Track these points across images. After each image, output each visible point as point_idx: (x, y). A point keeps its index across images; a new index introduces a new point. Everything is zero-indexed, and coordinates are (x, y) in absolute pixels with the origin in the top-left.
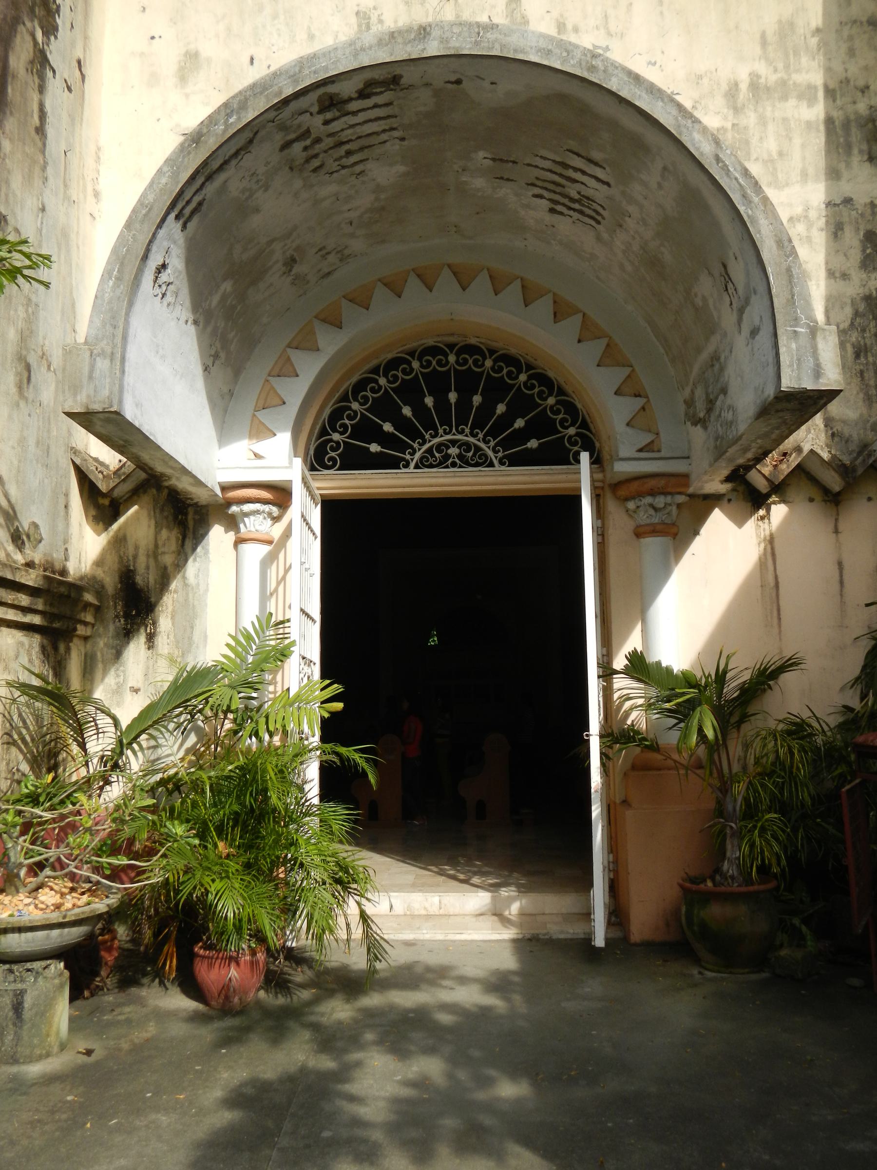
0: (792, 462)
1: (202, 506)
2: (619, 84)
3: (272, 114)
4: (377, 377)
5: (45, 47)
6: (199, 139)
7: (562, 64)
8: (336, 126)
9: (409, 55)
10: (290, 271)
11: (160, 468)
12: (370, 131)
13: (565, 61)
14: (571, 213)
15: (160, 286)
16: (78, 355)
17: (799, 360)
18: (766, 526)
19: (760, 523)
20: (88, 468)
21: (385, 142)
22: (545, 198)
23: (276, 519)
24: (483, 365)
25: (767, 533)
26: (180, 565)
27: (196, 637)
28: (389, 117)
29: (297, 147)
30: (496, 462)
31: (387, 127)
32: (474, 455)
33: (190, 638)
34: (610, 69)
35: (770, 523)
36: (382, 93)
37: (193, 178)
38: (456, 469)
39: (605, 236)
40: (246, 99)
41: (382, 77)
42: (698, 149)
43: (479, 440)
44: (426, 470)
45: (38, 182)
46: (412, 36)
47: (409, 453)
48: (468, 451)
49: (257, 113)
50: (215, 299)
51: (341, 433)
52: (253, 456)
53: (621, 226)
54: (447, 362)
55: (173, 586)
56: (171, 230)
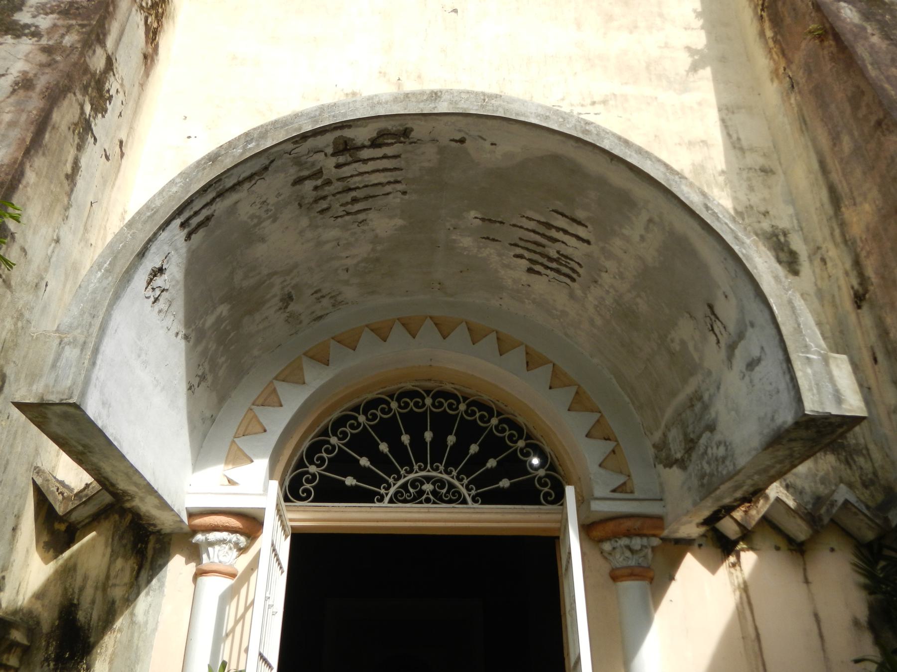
0: (761, 508)
1: (165, 534)
2: (611, 145)
3: (290, 146)
4: (357, 415)
5: (91, 119)
6: (216, 158)
8: (347, 171)
9: (422, 110)
10: (286, 307)
11: (122, 484)
12: (376, 182)
13: (560, 125)
14: (548, 272)
15: (153, 289)
16: (45, 342)
17: (817, 385)
18: (738, 573)
19: (732, 570)
20: (48, 487)
21: (388, 194)
22: (525, 258)
23: (242, 550)
24: (457, 408)
25: (741, 580)
26: (129, 600)
28: (395, 169)
29: (309, 185)
30: (469, 499)
31: (392, 180)
32: (448, 492)
34: (602, 134)
35: (741, 570)
36: (392, 144)
37: (204, 190)
38: (429, 505)
39: (579, 293)
40: (267, 131)
41: (394, 129)
42: (688, 198)
43: (453, 478)
44: (400, 505)
45: (57, 216)
46: (425, 98)
47: (384, 488)
48: (442, 487)
50: (210, 320)
51: (318, 466)
52: (227, 483)
53: (596, 282)
54: (424, 405)
55: (118, 624)
56: (174, 236)
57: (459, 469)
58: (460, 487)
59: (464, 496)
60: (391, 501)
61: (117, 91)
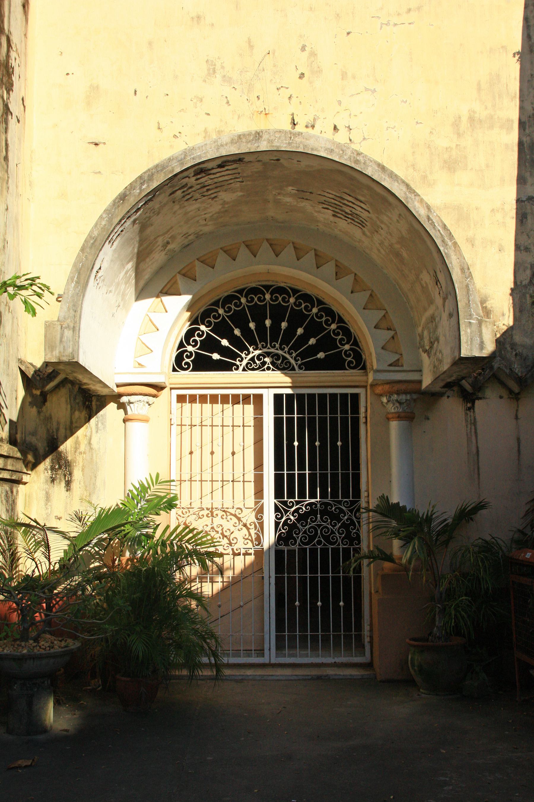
1: (102, 396)
4: (218, 309)
7: (341, 157)
9: (250, 149)
10: (166, 248)
14: (347, 219)
16: (54, 328)
17: (471, 339)
18: (472, 414)
19: (468, 412)
21: (231, 183)
22: (330, 210)
24: (288, 301)
27: (99, 483)
29: (179, 193)
30: (296, 367)
32: (282, 362)
33: (94, 484)
34: (368, 162)
35: (474, 412)
36: (232, 165)
38: (270, 372)
39: (368, 234)
40: (153, 174)
42: (417, 212)
43: (285, 353)
46: (251, 138)
47: (239, 360)
48: (278, 359)
49: (159, 183)
52: (137, 365)
54: (265, 299)
57: (290, 346)
58: (290, 359)
59: (293, 365)
60: (244, 370)
61: (15, 59)
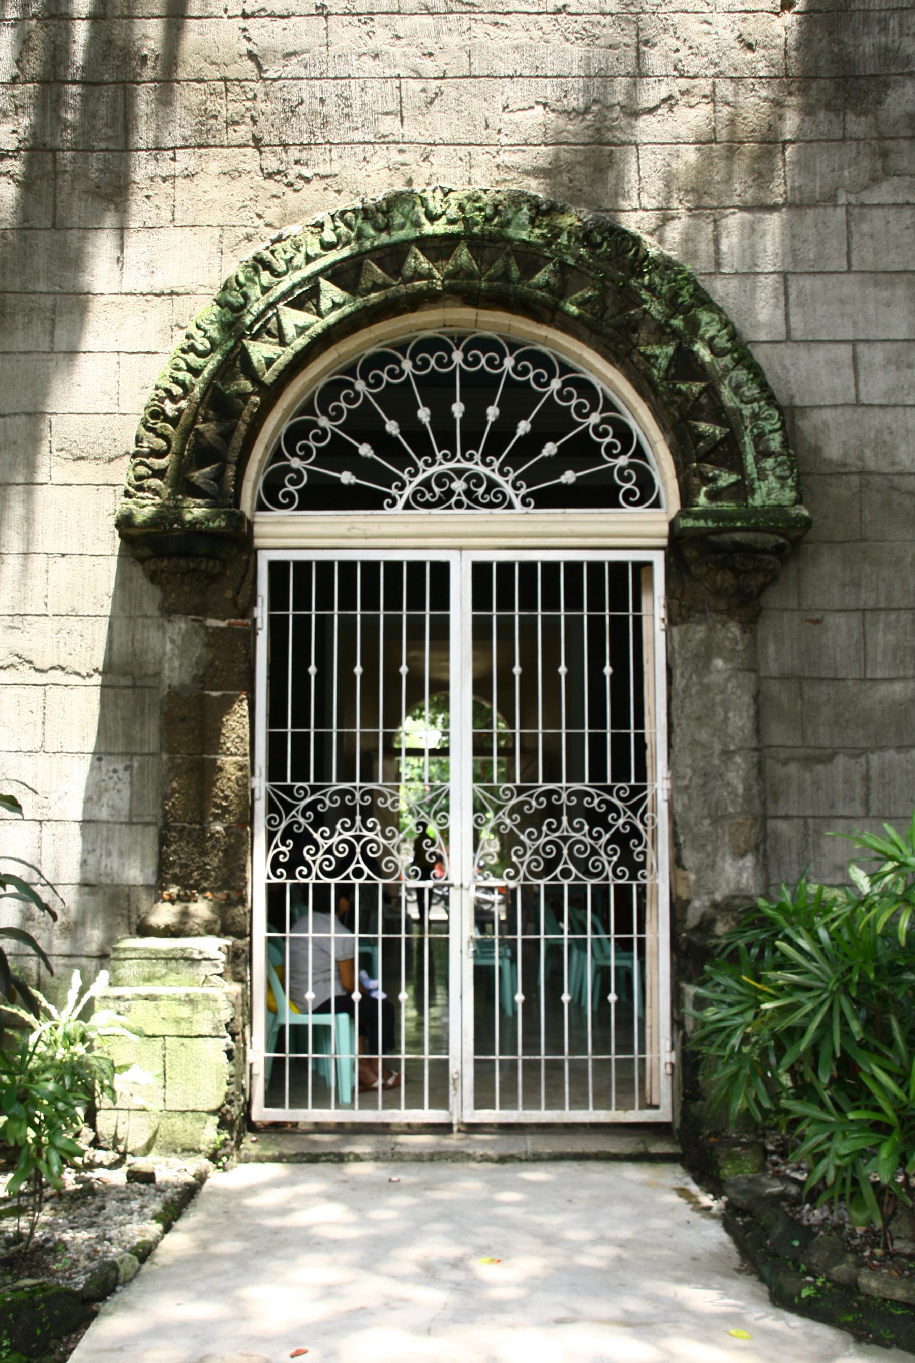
30: (517, 502)
32: (487, 491)
38: (462, 511)
47: (396, 487)
48: (478, 485)
60: (407, 506)
